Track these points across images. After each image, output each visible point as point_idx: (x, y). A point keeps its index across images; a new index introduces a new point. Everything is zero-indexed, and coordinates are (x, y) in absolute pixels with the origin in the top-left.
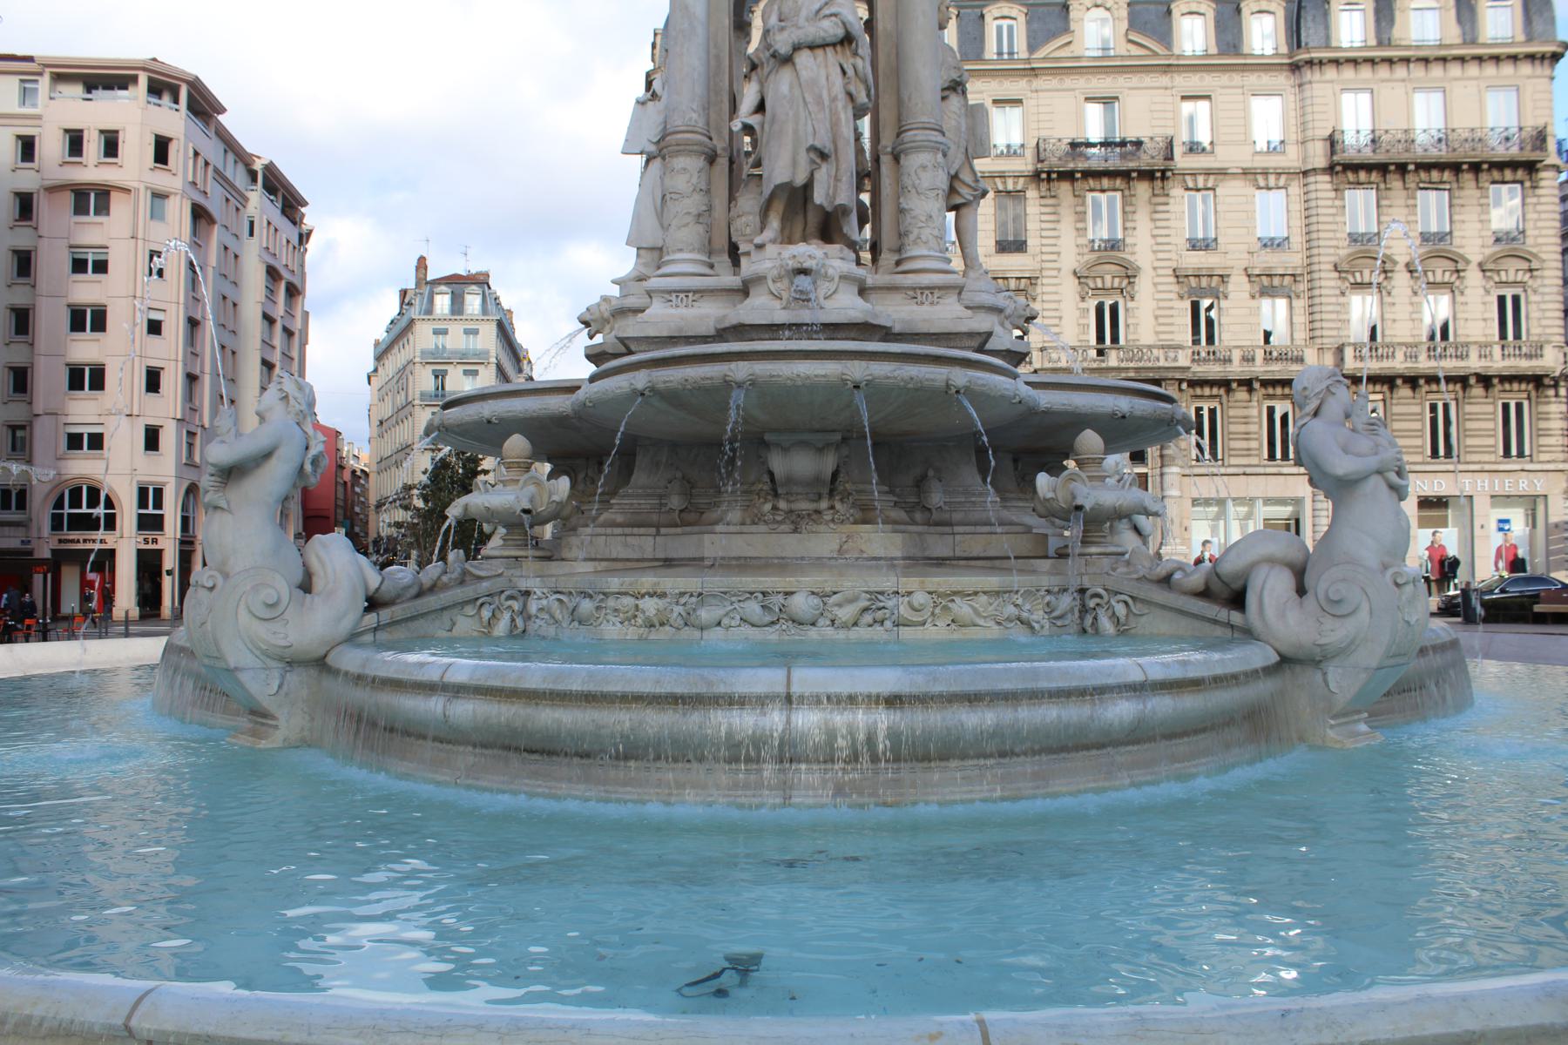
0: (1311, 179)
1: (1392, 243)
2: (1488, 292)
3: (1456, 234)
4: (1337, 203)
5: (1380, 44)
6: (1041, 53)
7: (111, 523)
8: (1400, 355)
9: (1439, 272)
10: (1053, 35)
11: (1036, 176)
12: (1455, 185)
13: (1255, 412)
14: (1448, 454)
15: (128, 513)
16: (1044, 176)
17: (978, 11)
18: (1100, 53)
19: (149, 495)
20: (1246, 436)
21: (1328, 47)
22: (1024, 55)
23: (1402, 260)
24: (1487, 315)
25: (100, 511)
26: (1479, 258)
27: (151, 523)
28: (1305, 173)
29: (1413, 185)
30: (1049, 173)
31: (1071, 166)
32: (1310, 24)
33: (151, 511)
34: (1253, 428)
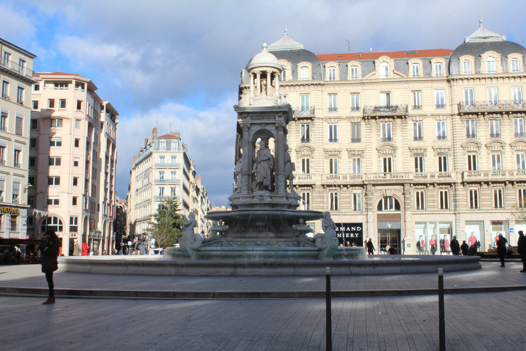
0: (454, 117)
1: (480, 138)
2: (513, 153)
3: (502, 134)
4: (462, 125)
5: (476, 73)
6: (365, 78)
7: (61, 229)
8: (482, 175)
9: (496, 147)
10: (370, 72)
11: (364, 118)
12: (501, 119)
13: (436, 193)
14: (501, 206)
15: (66, 226)
16: (366, 118)
17: (346, 64)
18: (385, 77)
19: (73, 220)
20: (433, 201)
21: (459, 75)
22: (360, 78)
23: (484, 143)
24: (512, 161)
25: (58, 225)
26: (510, 142)
27: (73, 229)
28: (452, 115)
29: (487, 119)
30: (368, 117)
31: (375, 115)
32: (453, 67)
33: (74, 225)
34: (435, 199)
